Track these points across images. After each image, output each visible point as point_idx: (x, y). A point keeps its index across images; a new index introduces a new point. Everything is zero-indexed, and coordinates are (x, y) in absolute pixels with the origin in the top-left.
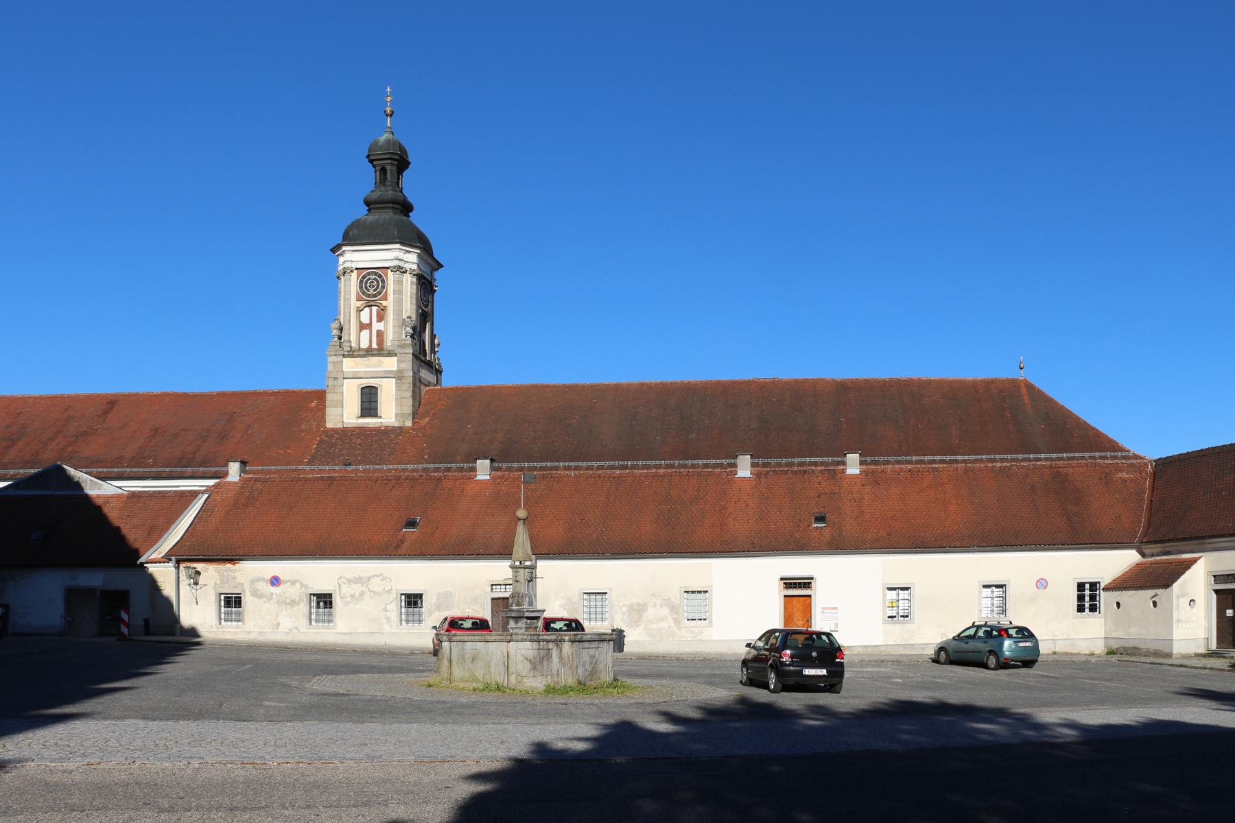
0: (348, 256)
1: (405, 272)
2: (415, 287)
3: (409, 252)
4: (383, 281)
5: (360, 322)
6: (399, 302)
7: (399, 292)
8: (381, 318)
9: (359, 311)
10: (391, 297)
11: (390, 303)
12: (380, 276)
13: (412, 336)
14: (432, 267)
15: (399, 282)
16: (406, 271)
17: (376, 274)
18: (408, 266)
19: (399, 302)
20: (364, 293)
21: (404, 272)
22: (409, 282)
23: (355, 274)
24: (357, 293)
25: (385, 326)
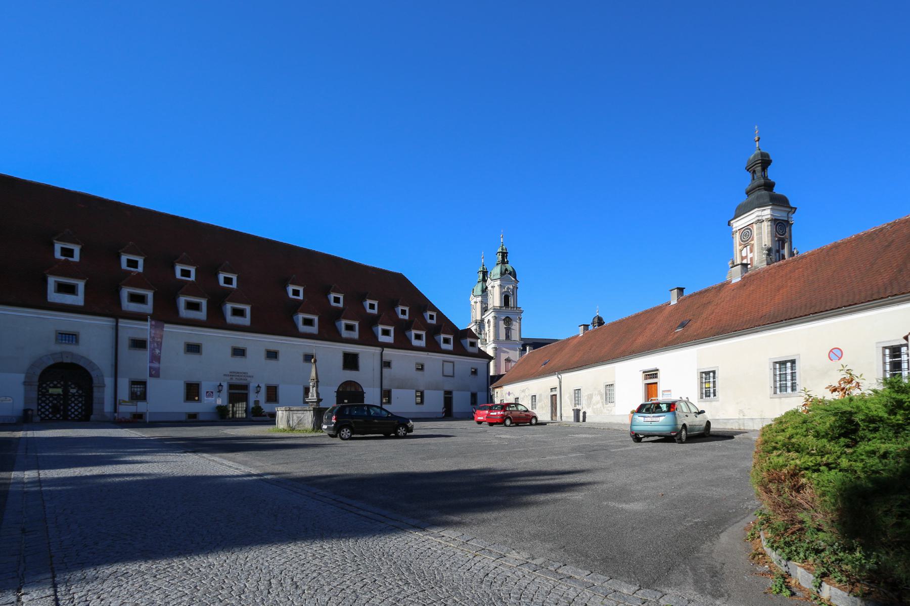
0: (734, 225)
1: (763, 221)
2: (770, 227)
3: (764, 210)
4: (751, 231)
5: (742, 257)
6: (760, 239)
7: (760, 234)
8: (751, 251)
9: (741, 251)
10: (755, 238)
11: (755, 242)
12: (750, 229)
13: (768, 255)
14: (787, 211)
15: (760, 228)
16: (763, 221)
17: (747, 229)
18: (764, 218)
19: (760, 239)
20: (742, 241)
21: (761, 222)
22: (766, 226)
23: (738, 234)
24: (740, 242)
25: (754, 255)
